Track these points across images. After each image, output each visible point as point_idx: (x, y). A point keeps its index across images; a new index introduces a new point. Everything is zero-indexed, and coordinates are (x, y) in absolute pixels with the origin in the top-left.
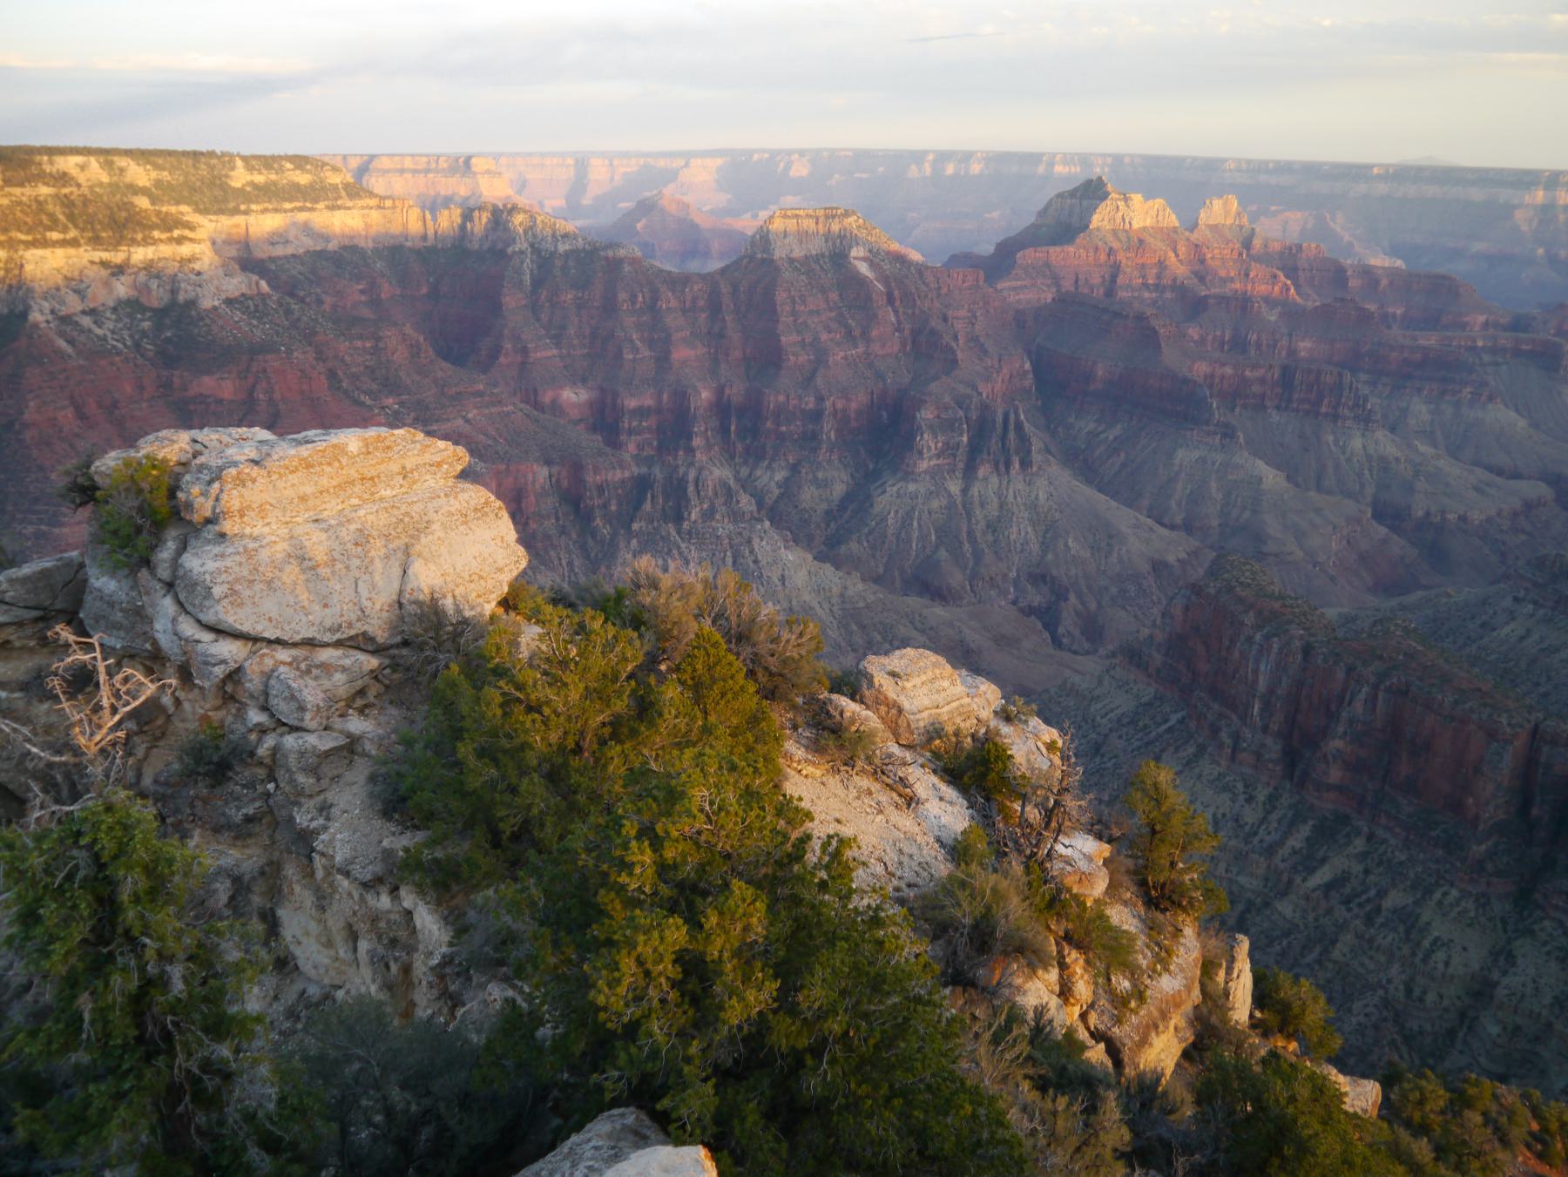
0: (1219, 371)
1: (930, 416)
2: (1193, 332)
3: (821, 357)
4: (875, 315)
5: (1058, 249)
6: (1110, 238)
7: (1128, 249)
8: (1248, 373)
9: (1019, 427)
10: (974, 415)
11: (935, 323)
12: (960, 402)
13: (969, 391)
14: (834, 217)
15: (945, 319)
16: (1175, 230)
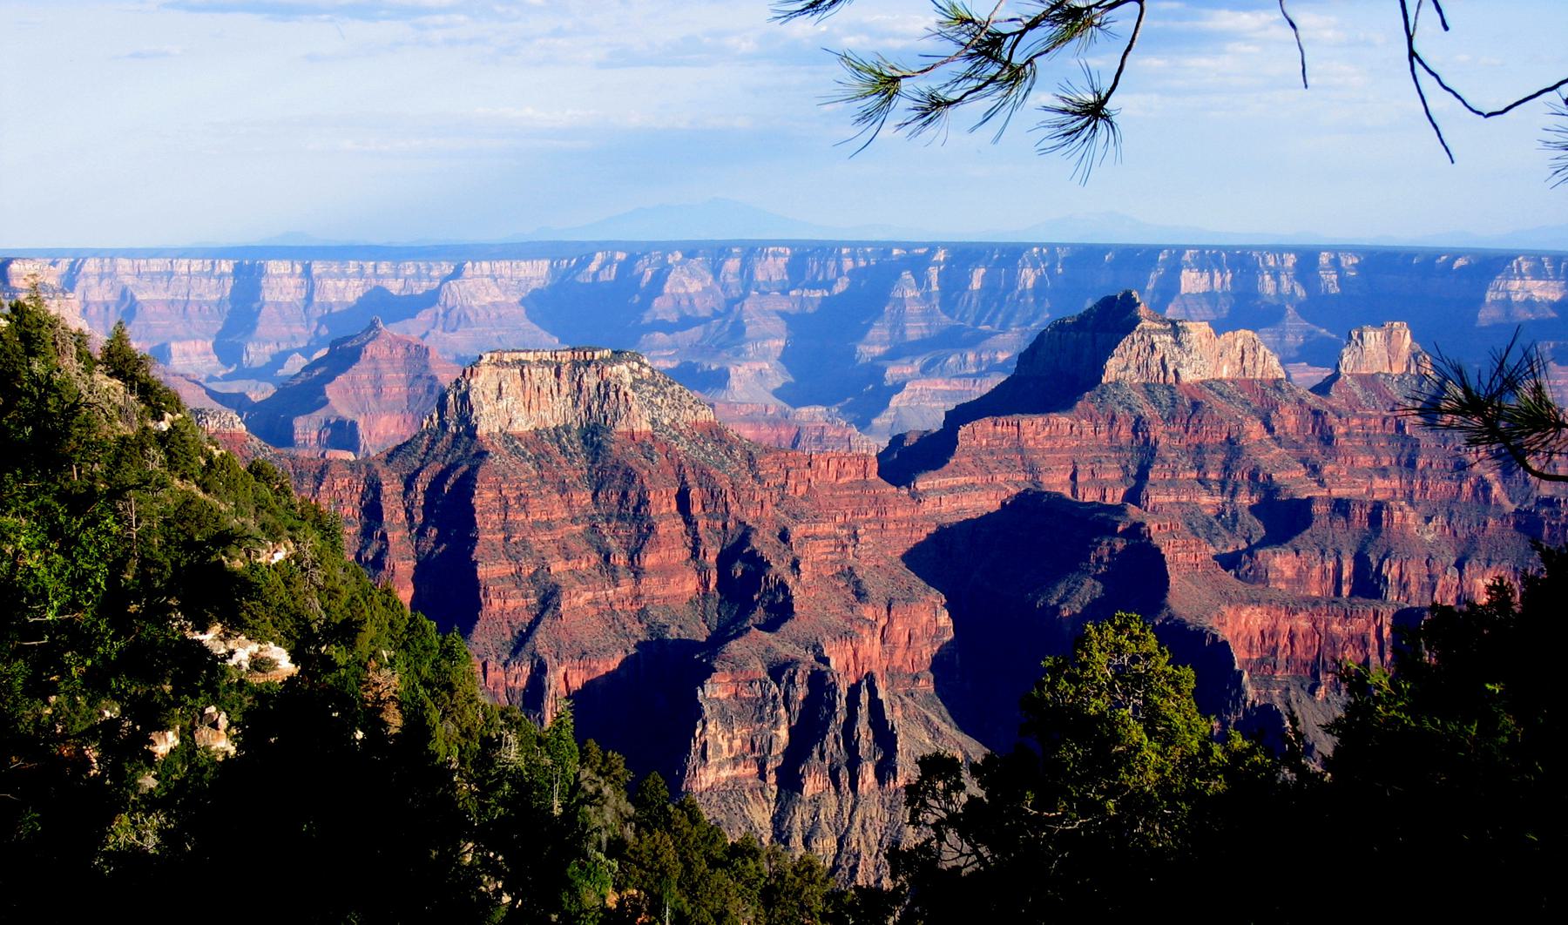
0: (1284, 626)
1: (723, 695)
2: (1281, 562)
3: (549, 599)
4: (650, 528)
5: (1039, 420)
6: (1138, 398)
7: (1172, 418)
8: (1336, 627)
9: (876, 706)
10: (801, 692)
11: (763, 543)
12: (778, 670)
13: (800, 653)
14: (588, 364)
15: (784, 536)
16: (1276, 384)
